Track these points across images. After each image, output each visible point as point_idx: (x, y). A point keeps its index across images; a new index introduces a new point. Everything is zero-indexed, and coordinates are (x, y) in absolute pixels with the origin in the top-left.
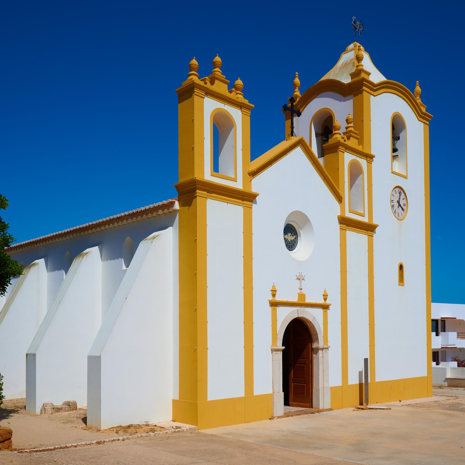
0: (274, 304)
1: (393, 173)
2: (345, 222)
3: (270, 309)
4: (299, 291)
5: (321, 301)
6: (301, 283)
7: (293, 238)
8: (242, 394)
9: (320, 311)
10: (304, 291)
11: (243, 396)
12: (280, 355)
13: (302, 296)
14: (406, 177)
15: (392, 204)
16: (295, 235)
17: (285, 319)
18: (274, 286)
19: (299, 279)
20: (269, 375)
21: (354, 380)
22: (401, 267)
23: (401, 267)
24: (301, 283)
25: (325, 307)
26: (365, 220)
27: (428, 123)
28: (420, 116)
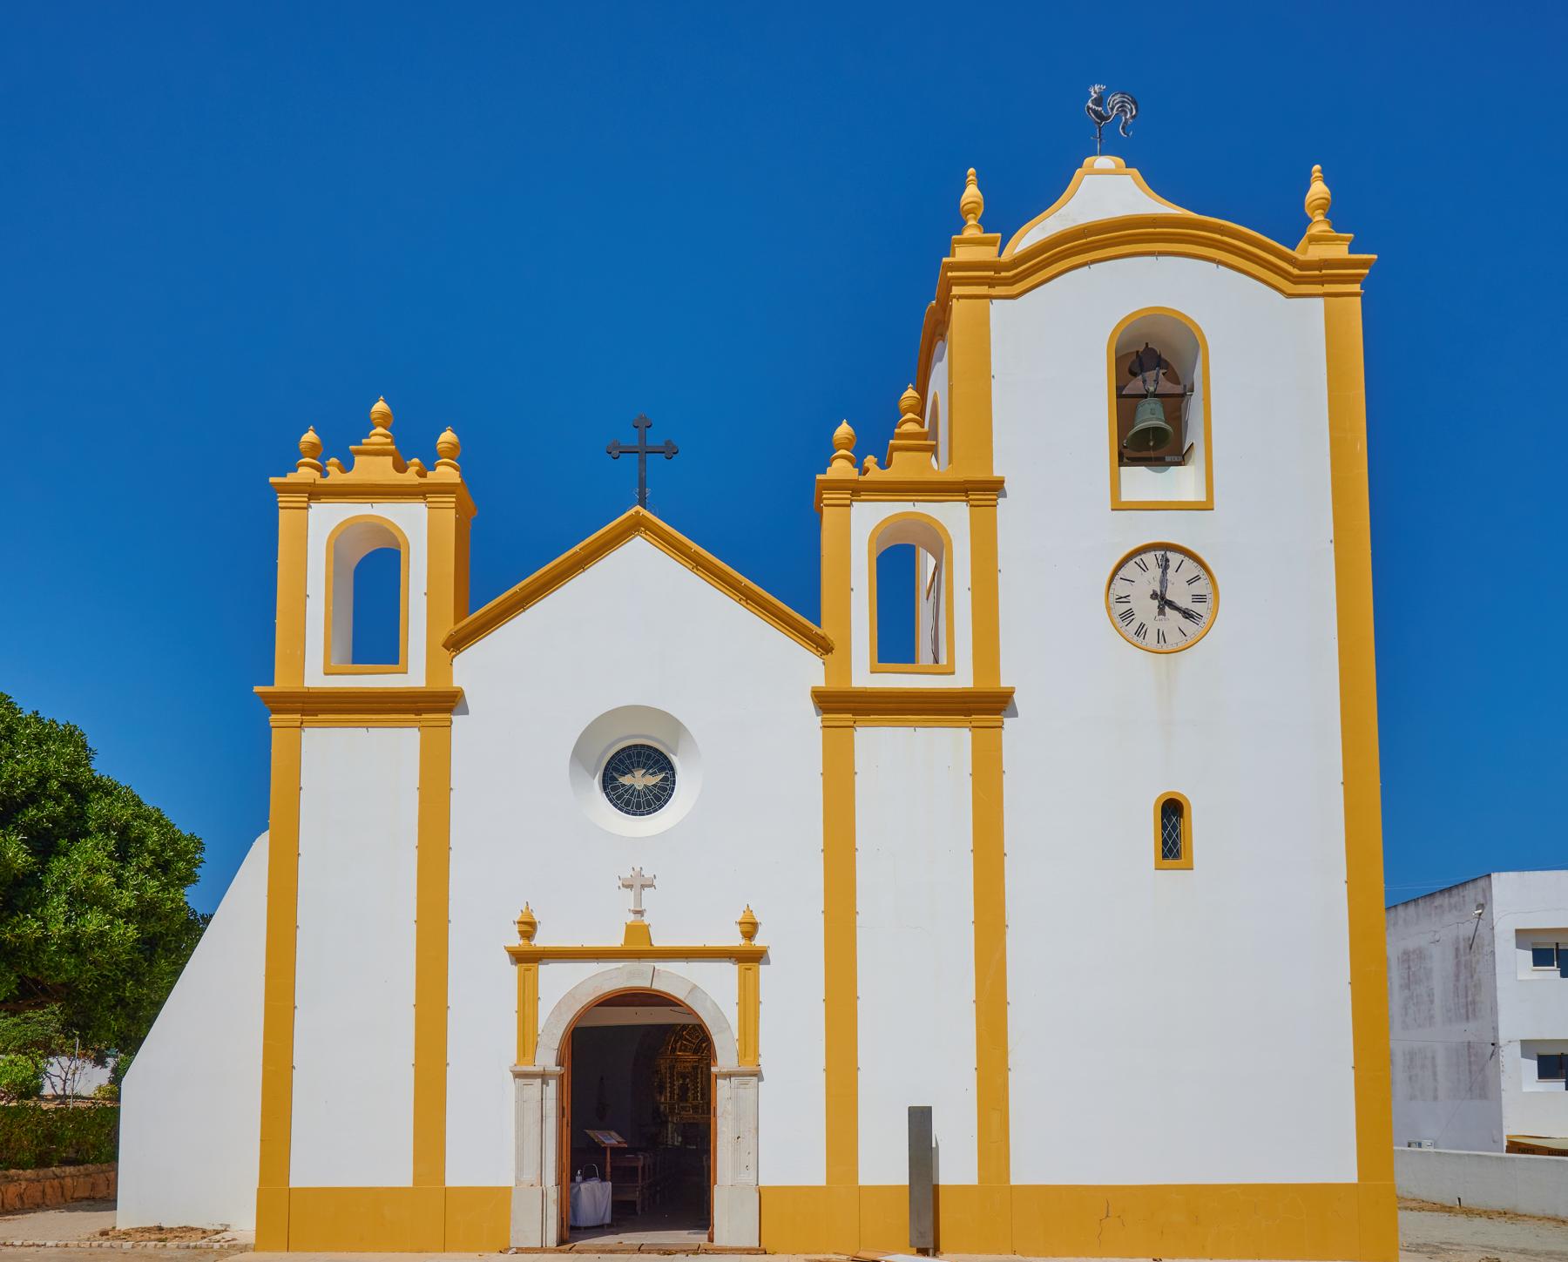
0: (526, 958)
1: (1119, 506)
2: (840, 705)
3: (514, 971)
4: (631, 918)
5: (735, 941)
6: (639, 900)
7: (652, 780)
8: (400, 1174)
9: (730, 970)
10: (646, 920)
11: (410, 1184)
12: (552, 1088)
13: (637, 931)
14: (1206, 506)
15: (1124, 607)
16: (661, 770)
17: (571, 995)
18: (528, 911)
19: (630, 887)
20: (505, 1138)
21: (884, 1162)
22: (1172, 810)
23: (1172, 810)
24: (639, 900)
25: (750, 958)
26: (962, 679)
27: (1356, 288)
28: (1297, 280)
